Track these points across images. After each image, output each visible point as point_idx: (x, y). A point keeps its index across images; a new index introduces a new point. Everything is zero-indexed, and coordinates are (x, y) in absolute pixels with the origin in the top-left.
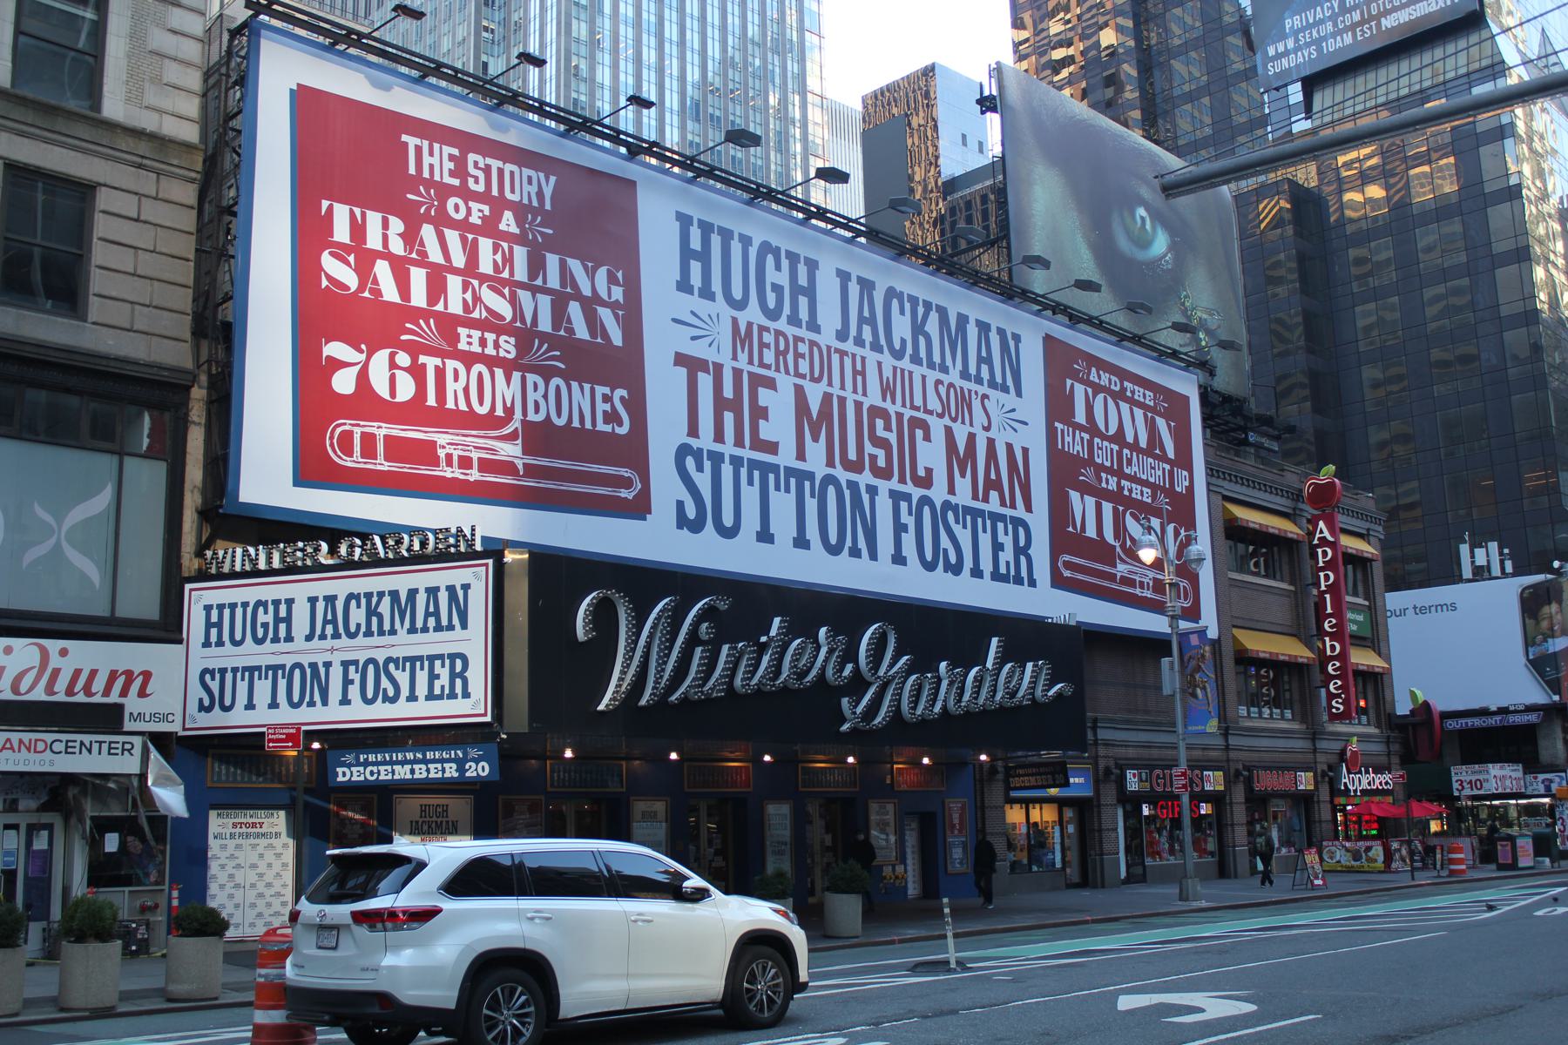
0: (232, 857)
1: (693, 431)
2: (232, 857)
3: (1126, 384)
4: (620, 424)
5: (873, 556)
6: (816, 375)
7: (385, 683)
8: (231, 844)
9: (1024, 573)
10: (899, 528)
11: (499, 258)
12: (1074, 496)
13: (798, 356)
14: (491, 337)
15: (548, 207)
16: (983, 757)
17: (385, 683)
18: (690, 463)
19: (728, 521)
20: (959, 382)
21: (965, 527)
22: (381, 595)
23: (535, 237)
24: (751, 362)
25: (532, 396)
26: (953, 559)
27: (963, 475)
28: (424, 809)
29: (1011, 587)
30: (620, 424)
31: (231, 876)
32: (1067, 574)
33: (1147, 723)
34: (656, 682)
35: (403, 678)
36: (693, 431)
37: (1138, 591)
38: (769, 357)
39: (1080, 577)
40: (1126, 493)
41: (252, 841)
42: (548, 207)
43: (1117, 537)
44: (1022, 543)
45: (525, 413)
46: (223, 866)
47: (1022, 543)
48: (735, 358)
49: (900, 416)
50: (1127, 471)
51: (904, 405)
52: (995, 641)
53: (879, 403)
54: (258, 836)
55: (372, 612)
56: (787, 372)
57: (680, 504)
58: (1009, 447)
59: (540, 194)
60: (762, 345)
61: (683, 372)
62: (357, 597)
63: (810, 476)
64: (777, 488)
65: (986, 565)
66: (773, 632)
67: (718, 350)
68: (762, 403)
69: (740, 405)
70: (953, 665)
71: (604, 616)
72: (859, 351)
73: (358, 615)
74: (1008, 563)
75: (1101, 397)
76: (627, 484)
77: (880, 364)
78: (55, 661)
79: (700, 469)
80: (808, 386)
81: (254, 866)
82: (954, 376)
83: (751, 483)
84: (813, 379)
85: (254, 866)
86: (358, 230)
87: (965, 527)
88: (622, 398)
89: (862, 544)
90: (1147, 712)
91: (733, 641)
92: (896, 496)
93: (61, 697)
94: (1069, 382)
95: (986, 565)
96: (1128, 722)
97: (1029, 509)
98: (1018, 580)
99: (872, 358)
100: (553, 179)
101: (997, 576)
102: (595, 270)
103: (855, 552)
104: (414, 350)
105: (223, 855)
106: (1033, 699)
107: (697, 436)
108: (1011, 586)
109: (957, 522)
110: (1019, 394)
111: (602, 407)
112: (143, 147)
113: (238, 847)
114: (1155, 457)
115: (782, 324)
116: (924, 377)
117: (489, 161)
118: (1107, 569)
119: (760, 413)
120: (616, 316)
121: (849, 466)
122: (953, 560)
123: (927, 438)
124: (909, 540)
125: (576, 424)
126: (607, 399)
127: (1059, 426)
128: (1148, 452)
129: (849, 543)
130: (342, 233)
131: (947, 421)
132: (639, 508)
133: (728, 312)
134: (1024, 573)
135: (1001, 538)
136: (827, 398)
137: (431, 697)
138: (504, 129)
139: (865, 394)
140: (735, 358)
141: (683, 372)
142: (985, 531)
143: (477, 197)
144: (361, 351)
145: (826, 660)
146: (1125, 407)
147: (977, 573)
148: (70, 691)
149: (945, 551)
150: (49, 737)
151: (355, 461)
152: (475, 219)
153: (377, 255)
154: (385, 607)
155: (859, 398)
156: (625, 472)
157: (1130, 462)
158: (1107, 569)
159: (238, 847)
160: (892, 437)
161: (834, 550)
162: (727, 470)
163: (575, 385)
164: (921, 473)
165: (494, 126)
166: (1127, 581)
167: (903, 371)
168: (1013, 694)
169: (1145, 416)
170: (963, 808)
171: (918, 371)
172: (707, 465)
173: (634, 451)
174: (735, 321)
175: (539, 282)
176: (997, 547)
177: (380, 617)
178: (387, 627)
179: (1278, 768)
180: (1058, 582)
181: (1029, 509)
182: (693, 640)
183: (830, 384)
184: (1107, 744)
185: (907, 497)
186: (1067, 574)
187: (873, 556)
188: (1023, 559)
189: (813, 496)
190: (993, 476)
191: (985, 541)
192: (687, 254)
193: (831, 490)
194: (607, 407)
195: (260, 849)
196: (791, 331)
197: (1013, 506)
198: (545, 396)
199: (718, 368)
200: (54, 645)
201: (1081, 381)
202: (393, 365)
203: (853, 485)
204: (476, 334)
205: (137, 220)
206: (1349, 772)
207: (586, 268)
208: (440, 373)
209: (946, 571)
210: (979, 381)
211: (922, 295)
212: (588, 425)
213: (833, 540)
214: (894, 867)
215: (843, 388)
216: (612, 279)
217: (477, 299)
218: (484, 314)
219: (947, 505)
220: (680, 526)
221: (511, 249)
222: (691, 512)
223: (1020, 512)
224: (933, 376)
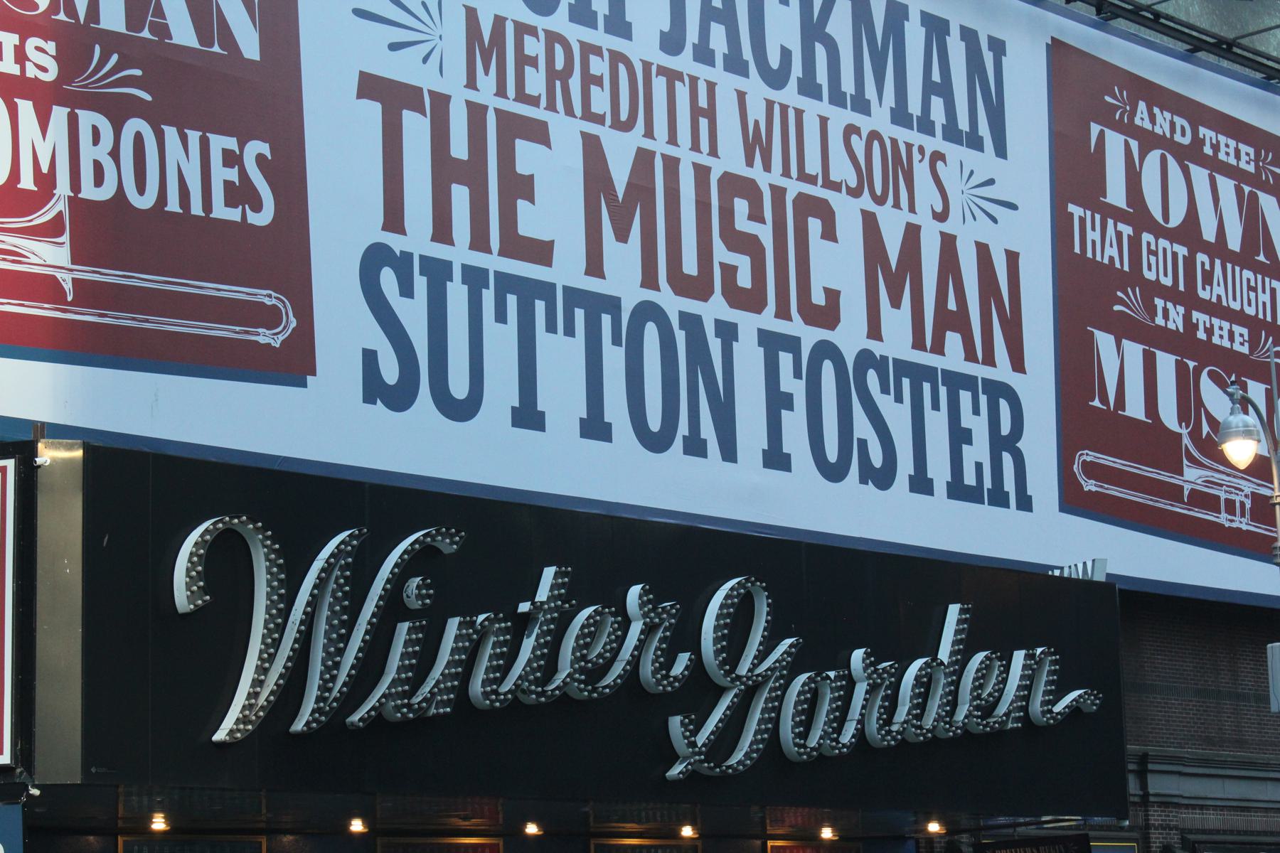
1: (394, 219)
3: (1203, 131)
4: (257, 207)
6: (624, 116)
9: (1009, 485)
10: (777, 402)
12: (1104, 341)
13: (589, 80)
16: (934, 827)
18: (388, 279)
19: (459, 387)
20: (890, 131)
21: (899, 399)
24: (501, 92)
25: (88, 154)
26: (877, 459)
27: (896, 304)
29: (985, 512)
30: (257, 207)
32: (1090, 486)
34: (324, 688)
36: (394, 219)
37: (1223, 518)
38: (536, 82)
39: (1114, 491)
40: (1201, 335)
43: (1183, 417)
44: (1005, 429)
47: (1005, 429)
48: (471, 84)
50: (1204, 294)
51: (786, 173)
52: (954, 611)
56: (569, 111)
57: (370, 358)
63: (613, 305)
64: (551, 328)
65: (939, 470)
66: (542, 594)
67: (440, 68)
68: (522, 168)
69: (483, 172)
70: (876, 655)
71: (227, 564)
72: (702, 72)
74: (979, 466)
75: (1154, 157)
76: (270, 318)
77: (741, 96)
79: (407, 290)
80: (606, 135)
82: (880, 119)
83: (501, 317)
84: (618, 125)
87: (899, 399)
88: (260, 159)
89: (708, 430)
90: (1240, 743)
91: (468, 611)
92: (772, 343)
94: (1095, 129)
95: (939, 470)
96: (1205, 762)
97: (1018, 364)
98: (999, 498)
101: (957, 490)
103: (695, 447)
106: (1026, 719)
107: (402, 232)
109: (885, 390)
111: (222, 174)
114: (1257, 268)
116: (824, 121)
118: (1165, 477)
119: (519, 187)
121: (682, 285)
122: (877, 459)
123: (829, 233)
124: (794, 424)
125: (173, 205)
126: (231, 159)
127: (1076, 210)
128: (1244, 259)
129: (683, 429)
131: (866, 202)
132: (293, 364)
134: (1009, 485)
135: (967, 420)
136: (643, 159)
139: (713, 152)
140: (471, 84)
142: (936, 406)
145: (641, 646)
146: (1200, 175)
147: (921, 484)
149: (863, 444)
155: (704, 159)
156: (266, 297)
157: (1208, 278)
158: (1165, 477)
160: (765, 234)
161: (656, 442)
163: (171, 133)
164: (818, 298)
166: (1200, 499)
168: (988, 709)
169: (1239, 191)
172: (420, 284)
173: (282, 256)
176: (960, 437)
180: (1073, 500)
181: (1018, 364)
182: (393, 608)
183: (649, 133)
184: (1168, 803)
185: (793, 344)
186: (1090, 486)
187: (729, 454)
188: (1007, 459)
189: (616, 341)
190: (952, 305)
191: (937, 423)
193: (651, 332)
194: (233, 175)
196: (576, 34)
197: (989, 360)
198: (115, 154)
199: (441, 103)
201: (1118, 127)
209: (863, 480)
210: (926, 126)
212: (197, 209)
215: (673, 140)
219: (865, 359)
220: (369, 398)
222: (390, 372)
223: (1002, 372)
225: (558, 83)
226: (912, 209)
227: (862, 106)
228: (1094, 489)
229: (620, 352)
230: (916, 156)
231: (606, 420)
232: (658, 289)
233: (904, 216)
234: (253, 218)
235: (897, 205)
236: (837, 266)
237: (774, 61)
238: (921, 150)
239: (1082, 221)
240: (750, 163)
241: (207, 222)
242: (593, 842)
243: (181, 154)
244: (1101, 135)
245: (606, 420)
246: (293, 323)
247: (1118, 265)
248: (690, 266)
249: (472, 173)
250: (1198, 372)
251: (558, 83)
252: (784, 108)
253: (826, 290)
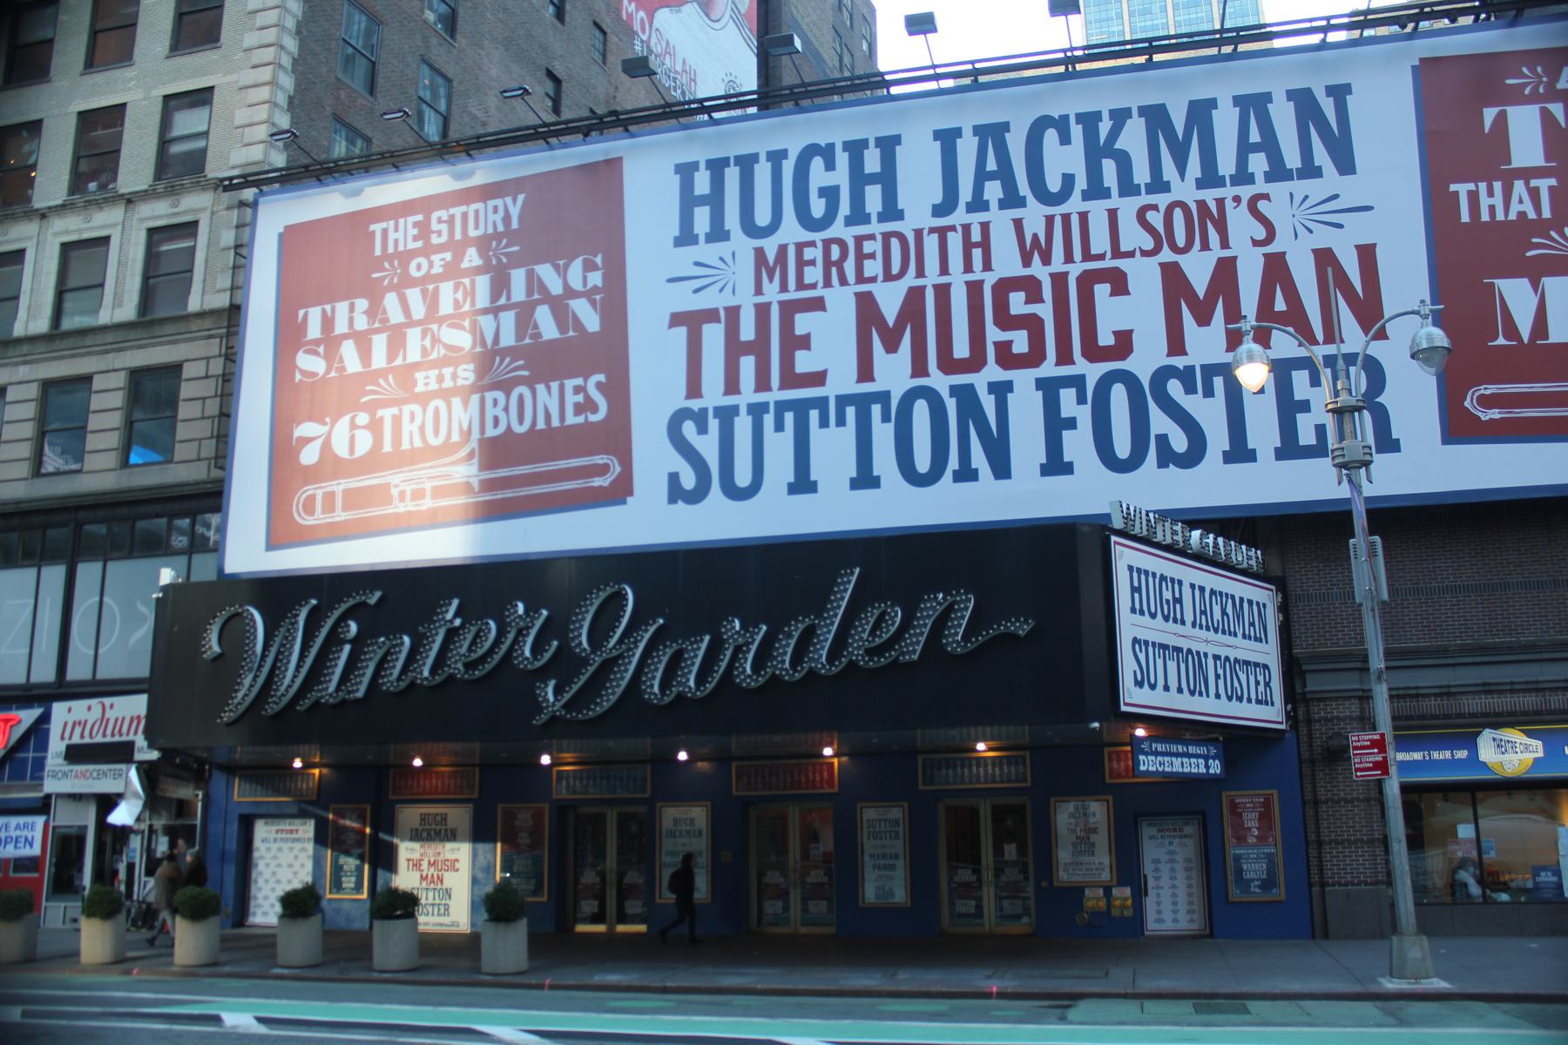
0: (275, 857)
1: (694, 390)
2: (275, 857)
4: (595, 409)
5: (1002, 469)
6: (895, 270)
8: (274, 846)
11: (460, 295)
13: (861, 257)
14: (448, 371)
15: (515, 225)
18: (689, 429)
19: (743, 478)
23: (499, 260)
24: (784, 288)
25: (490, 412)
26: (1179, 443)
28: (423, 818)
30: (595, 409)
31: (274, 873)
33: (1509, 649)
36: (694, 390)
38: (813, 274)
41: (290, 845)
42: (515, 225)
45: (482, 430)
46: (268, 865)
48: (759, 291)
49: (1059, 280)
51: (1069, 258)
53: (1017, 270)
54: (294, 840)
56: (843, 281)
57: (674, 478)
58: (1325, 258)
59: (507, 218)
60: (801, 264)
61: (682, 332)
63: (883, 397)
64: (824, 423)
69: (770, 344)
72: (976, 219)
77: (1018, 224)
78: (109, 713)
81: (290, 866)
83: (779, 427)
84: (888, 277)
85: (290, 866)
86: (328, 322)
87: (1209, 392)
88: (599, 385)
89: (979, 458)
92: (1049, 388)
93: (109, 739)
94: (1489, 114)
99: (1001, 221)
100: (521, 197)
101: (1289, 449)
102: (567, 266)
103: (966, 474)
104: (371, 408)
105: (268, 855)
109: (1190, 389)
110: (1346, 165)
111: (572, 399)
112: (207, 323)
113: (280, 849)
115: (838, 229)
116: (1113, 214)
117: (452, 211)
119: (795, 343)
120: (593, 303)
121: (949, 365)
122: (1179, 443)
125: (541, 425)
126: (577, 390)
129: (953, 463)
130: (314, 331)
132: (620, 491)
133: (742, 245)
136: (915, 295)
138: (470, 174)
139: (987, 266)
140: (759, 291)
141: (682, 332)
143: (441, 248)
144: (325, 423)
148: (113, 735)
149: (1163, 440)
150: (91, 767)
151: (319, 518)
152: (437, 269)
153: (345, 337)
156: (599, 459)
159: (280, 849)
160: (1045, 311)
162: (743, 426)
163: (541, 388)
164: (1105, 339)
165: (458, 177)
167: (1066, 218)
170: (1267, 804)
171: (1097, 211)
173: (614, 436)
174: (760, 253)
175: (503, 301)
180: (1458, 427)
182: (334, 640)
183: (920, 273)
185: (1078, 382)
189: (886, 418)
192: (688, 201)
193: (921, 409)
194: (580, 398)
195: (295, 852)
198: (506, 409)
199: (733, 313)
200: (107, 701)
202: (353, 426)
203: (965, 395)
204: (433, 373)
205: (207, 377)
207: (557, 268)
208: (397, 421)
209: (1162, 463)
211: (1104, 105)
213: (923, 463)
214: (1108, 891)
215: (944, 270)
216: (589, 267)
217: (436, 340)
218: (443, 351)
219: (1162, 376)
220: (672, 500)
221: (473, 283)
222: (689, 481)
224: (1127, 208)
225: (834, 270)
226: (1225, 244)
227: (1158, 184)
228: (1497, 416)
229: (890, 427)
230: (1229, 204)
231: (875, 473)
232: (927, 375)
233: (1217, 252)
234: (593, 418)
235: (1205, 246)
236: (1135, 311)
237: (1054, 185)
238: (1237, 199)
239: (1473, 197)
240: (1027, 263)
241: (564, 429)
242: (920, 759)
243: (547, 397)
244: (1501, 120)
245: (875, 473)
246: (618, 469)
247: (1532, 215)
248: (961, 349)
249: (759, 347)
251: (834, 270)
252: (1066, 218)
253: (1116, 333)
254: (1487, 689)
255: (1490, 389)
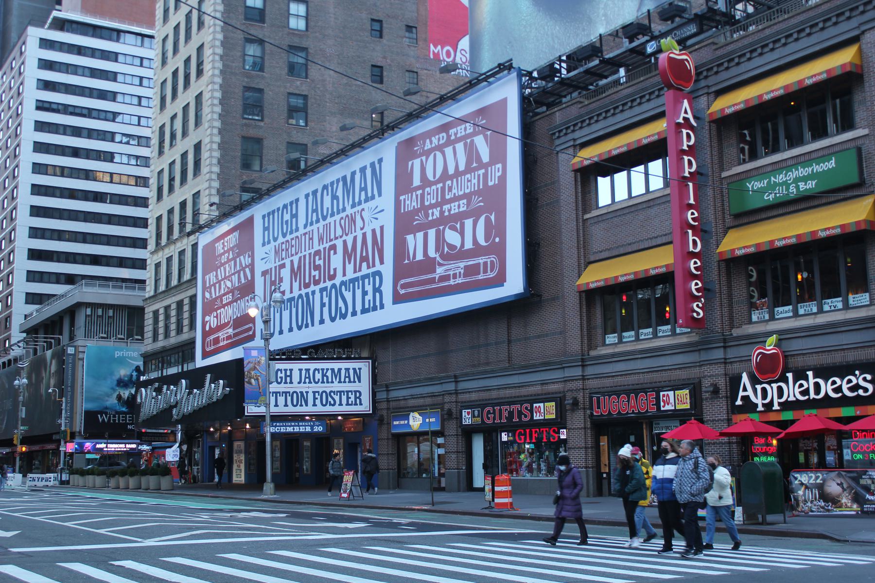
7: (330, 399)
17: (330, 399)
22: (327, 370)
27: (350, 263)
29: (372, 314)
35: (337, 398)
37: (452, 282)
39: (411, 290)
55: (324, 375)
62: (318, 370)
73: (318, 376)
90: (488, 364)
108: (371, 313)
118: (429, 276)
122: (343, 312)
123: (335, 253)
124: (326, 309)
134: (378, 303)
137: (348, 404)
154: (329, 374)
158: (429, 276)
176: (365, 293)
177: (327, 377)
178: (330, 380)
179: (628, 393)
181: (382, 262)
188: (378, 295)
190: (364, 254)
206: (754, 381)
250: (444, 229)
254: (413, 397)
255: (402, 282)
